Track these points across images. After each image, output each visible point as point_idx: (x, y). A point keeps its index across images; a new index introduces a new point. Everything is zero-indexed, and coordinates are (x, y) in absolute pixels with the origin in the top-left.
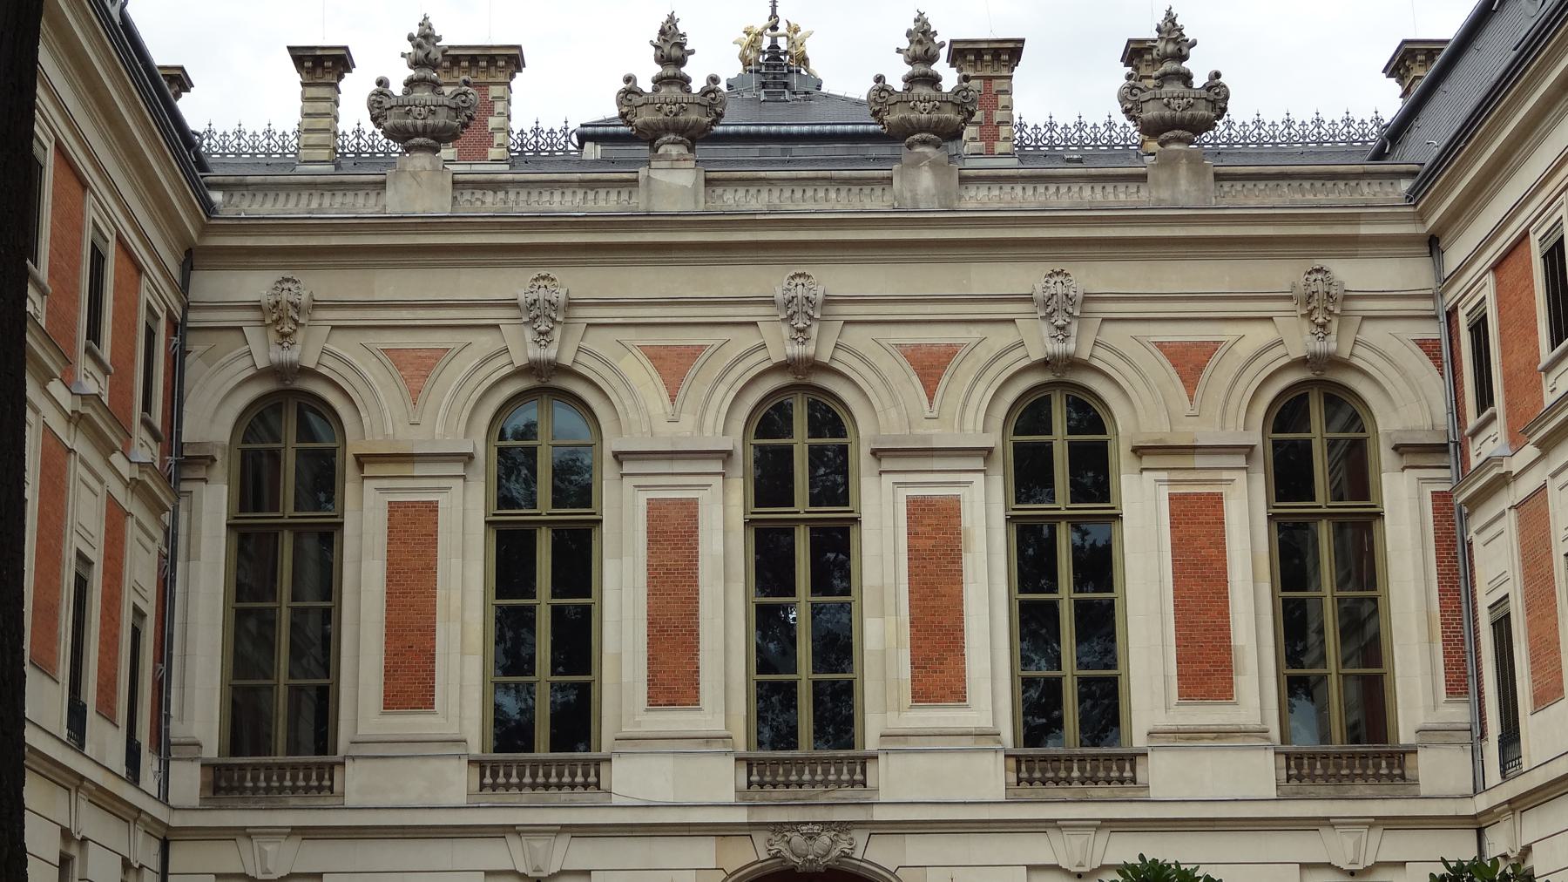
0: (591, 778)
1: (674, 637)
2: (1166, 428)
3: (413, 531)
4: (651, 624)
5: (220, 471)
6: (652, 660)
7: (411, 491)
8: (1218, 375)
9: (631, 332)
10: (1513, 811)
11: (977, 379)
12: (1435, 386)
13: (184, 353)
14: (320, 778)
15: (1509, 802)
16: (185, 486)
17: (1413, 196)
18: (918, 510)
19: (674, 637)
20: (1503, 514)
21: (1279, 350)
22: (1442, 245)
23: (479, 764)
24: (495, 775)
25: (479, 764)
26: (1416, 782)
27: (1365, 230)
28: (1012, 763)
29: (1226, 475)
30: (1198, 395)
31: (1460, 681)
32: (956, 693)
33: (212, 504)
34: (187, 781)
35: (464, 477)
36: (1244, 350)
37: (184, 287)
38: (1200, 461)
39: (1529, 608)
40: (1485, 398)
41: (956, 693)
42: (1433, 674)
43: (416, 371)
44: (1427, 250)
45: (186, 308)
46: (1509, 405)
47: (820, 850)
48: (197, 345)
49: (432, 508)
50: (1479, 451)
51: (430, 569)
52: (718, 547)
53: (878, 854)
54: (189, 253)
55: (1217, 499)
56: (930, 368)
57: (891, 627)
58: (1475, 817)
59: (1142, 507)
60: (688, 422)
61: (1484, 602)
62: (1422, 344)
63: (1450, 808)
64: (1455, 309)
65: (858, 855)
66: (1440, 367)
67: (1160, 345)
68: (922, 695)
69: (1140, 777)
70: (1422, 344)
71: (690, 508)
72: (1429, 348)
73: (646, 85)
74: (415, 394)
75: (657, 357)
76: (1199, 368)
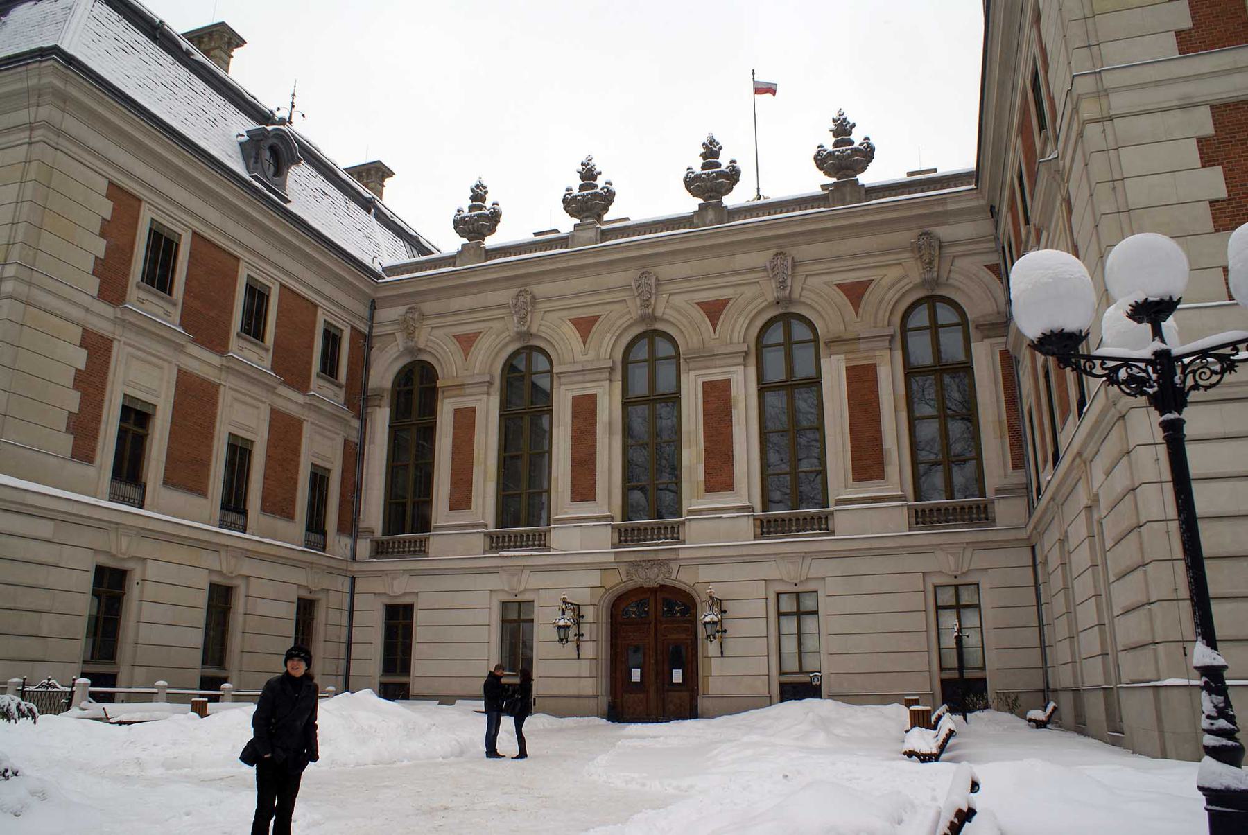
0: (540, 542)
1: (584, 464)
2: (842, 328)
3: (465, 420)
4: (573, 460)
5: (386, 400)
6: (573, 478)
7: (464, 403)
8: (869, 298)
9: (565, 313)
11: (739, 315)
13: (370, 348)
14: (420, 549)
16: (369, 410)
18: (709, 388)
19: (584, 464)
21: (906, 281)
23: (489, 536)
24: (497, 542)
25: (489, 536)
26: (994, 520)
27: (950, 207)
28: (758, 523)
29: (878, 353)
30: (861, 310)
31: (1019, 461)
32: (729, 486)
33: (381, 418)
34: (364, 547)
35: (488, 394)
36: (885, 282)
37: (372, 318)
38: (862, 346)
41: (729, 486)
42: (1004, 456)
43: (467, 342)
45: (371, 328)
47: (653, 578)
48: (377, 344)
49: (473, 410)
51: (472, 440)
52: (606, 418)
53: (684, 579)
54: (373, 302)
55: (873, 368)
56: (714, 310)
57: (694, 453)
58: (1029, 538)
59: (834, 374)
60: (592, 354)
62: (988, 267)
63: (1011, 535)
65: (673, 577)
66: (1000, 279)
67: (839, 286)
68: (710, 488)
69: (830, 527)
70: (988, 267)
71: (592, 398)
73: (576, 192)
74: (466, 356)
75: (576, 322)
76: (860, 297)
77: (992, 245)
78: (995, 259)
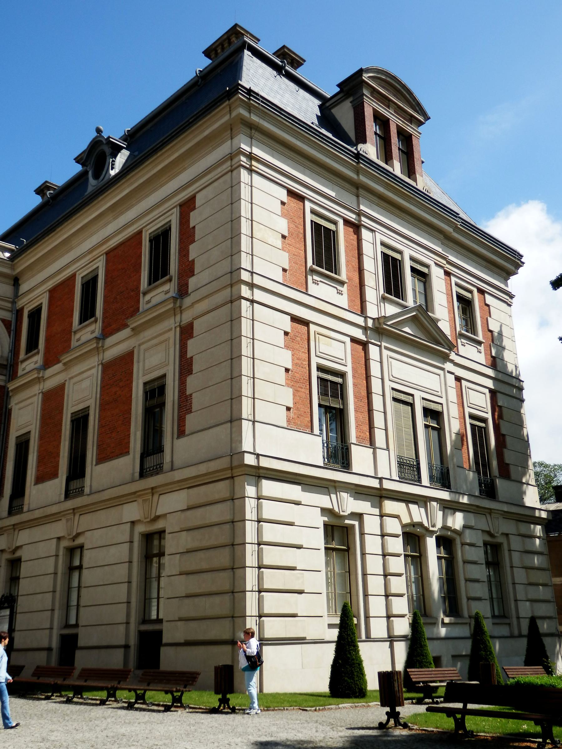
10: (14, 530)
12: (6, 341)
15: (14, 525)
17: (11, 259)
20: (35, 395)
22: (20, 282)
39: (41, 437)
40: (32, 345)
44: (13, 283)
46: (47, 348)
50: (23, 368)
61: (14, 434)
62: (3, 321)
64: (22, 309)
70: (3, 321)
72: (7, 324)
77: (9, 305)
78: (7, 316)
